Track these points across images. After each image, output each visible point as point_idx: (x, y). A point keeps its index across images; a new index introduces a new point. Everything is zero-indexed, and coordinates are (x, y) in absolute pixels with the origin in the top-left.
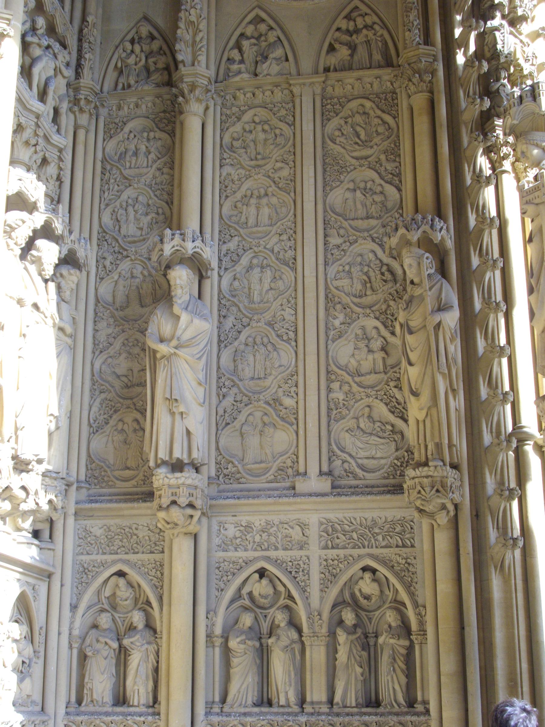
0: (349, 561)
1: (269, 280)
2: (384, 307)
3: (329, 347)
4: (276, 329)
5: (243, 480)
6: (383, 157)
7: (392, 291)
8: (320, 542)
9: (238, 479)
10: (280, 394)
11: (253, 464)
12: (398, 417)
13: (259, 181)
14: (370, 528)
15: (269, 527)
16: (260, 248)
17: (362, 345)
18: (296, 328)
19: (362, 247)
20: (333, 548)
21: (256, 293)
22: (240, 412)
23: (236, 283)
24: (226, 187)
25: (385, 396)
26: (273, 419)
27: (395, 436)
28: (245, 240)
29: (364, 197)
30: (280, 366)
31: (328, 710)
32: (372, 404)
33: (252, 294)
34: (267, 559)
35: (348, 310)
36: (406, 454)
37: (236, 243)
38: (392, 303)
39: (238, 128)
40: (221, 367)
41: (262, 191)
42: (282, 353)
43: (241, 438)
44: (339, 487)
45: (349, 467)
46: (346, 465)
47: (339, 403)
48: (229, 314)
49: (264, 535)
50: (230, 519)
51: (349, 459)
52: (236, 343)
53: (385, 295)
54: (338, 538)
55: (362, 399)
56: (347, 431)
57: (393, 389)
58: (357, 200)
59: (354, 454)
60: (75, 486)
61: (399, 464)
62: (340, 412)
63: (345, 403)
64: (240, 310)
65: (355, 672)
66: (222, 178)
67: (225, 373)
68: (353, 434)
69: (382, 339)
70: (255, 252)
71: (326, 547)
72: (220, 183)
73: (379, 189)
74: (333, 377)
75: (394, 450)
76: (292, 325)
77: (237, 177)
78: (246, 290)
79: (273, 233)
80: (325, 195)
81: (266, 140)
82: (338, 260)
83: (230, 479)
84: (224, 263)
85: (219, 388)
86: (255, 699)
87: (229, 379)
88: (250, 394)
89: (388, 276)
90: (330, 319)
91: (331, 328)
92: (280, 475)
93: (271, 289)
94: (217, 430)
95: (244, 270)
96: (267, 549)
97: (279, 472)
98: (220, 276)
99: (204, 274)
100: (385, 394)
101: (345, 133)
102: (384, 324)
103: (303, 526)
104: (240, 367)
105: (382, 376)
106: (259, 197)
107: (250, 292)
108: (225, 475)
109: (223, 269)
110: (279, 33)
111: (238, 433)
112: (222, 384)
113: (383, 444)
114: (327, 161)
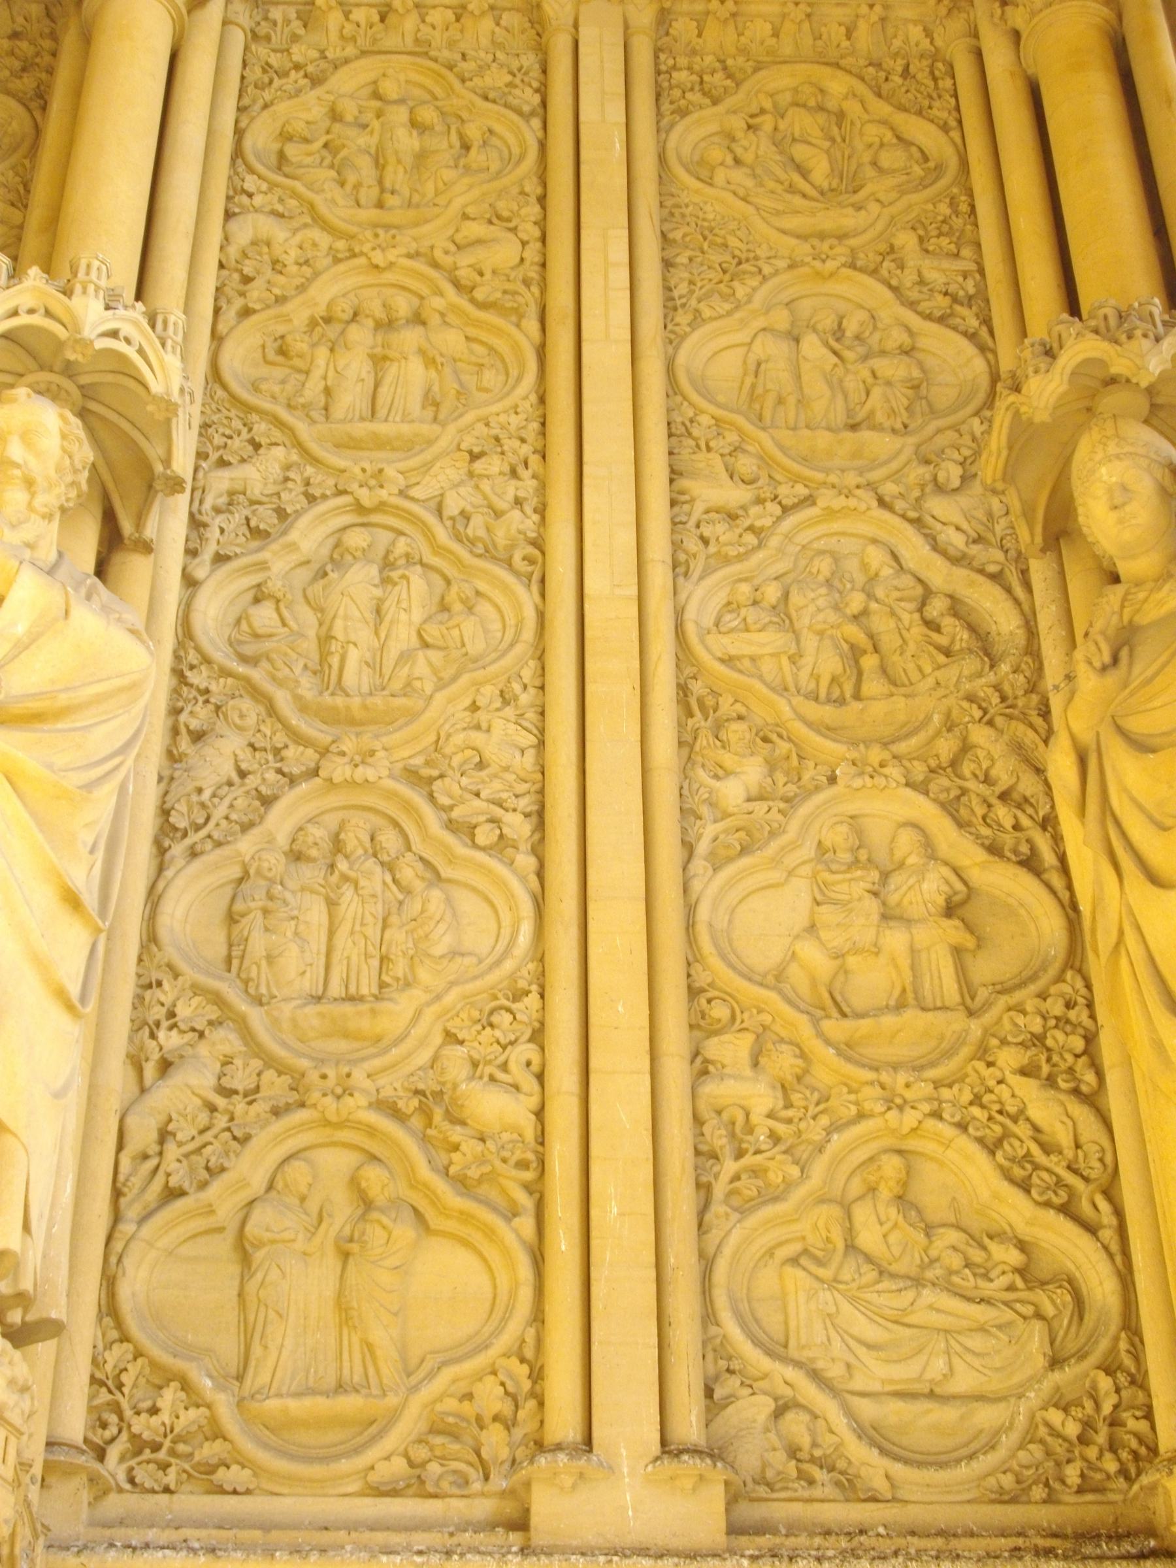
1: (417, 616)
2: (946, 747)
3: (696, 885)
4: (444, 800)
6: (907, 241)
7: (982, 687)
9: (211, 1469)
11: (298, 1395)
12: (1047, 1204)
13: (388, 277)
16: (383, 494)
17: (856, 886)
18: (542, 806)
19: (836, 526)
21: (354, 655)
22: (244, 1140)
23: (264, 616)
24: (247, 280)
25: (976, 1111)
26: (414, 1183)
27: (1041, 1297)
28: (315, 461)
29: (835, 359)
30: (455, 953)
32: (912, 1144)
33: (335, 661)
35: (783, 747)
36: (1105, 1383)
37: (276, 471)
38: (980, 735)
40: (163, 934)
42: (468, 904)
43: (235, 1269)
44: (760, 1529)
45: (812, 1432)
46: (795, 1425)
47: (750, 1129)
48: (221, 726)
51: (809, 1392)
52: (246, 845)
53: (951, 701)
55: (861, 1116)
56: (794, 1261)
57: (1015, 1080)
58: (805, 367)
59: (835, 1372)
61: (1072, 1429)
62: (756, 1172)
63: (781, 1129)
64: (272, 711)
66: (233, 251)
67: (182, 966)
68: (821, 1272)
69: (946, 872)
70: (359, 508)
72: (221, 266)
73: (898, 337)
74: (720, 1012)
75: (1041, 1362)
76: (524, 787)
77: (294, 253)
78: (310, 646)
79: (443, 443)
80: (673, 340)
81: (421, 157)
82: (727, 561)
83: (164, 1467)
84: (213, 534)
85: (144, 1027)
87: (197, 989)
88: (304, 1063)
89: (955, 632)
90: (702, 775)
91: (704, 810)
92: (443, 1459)
93: (426, 645)
94: (117, 1217)
95: (304, 574)
97: (438, 1440)
98: (190, 582)
99: (127, 526)
100: (977, 1100)
101: (748, 158)
102: (951, 808)
104: (258, 944)
105: (957, 1022)
106: (386, 325)
107: (324, 656)
108: (139, 1445)
109: (207, 555)
111: (223, 1245)
112: (158, 1013)
113: (982, 1329)
114: (677, 235)
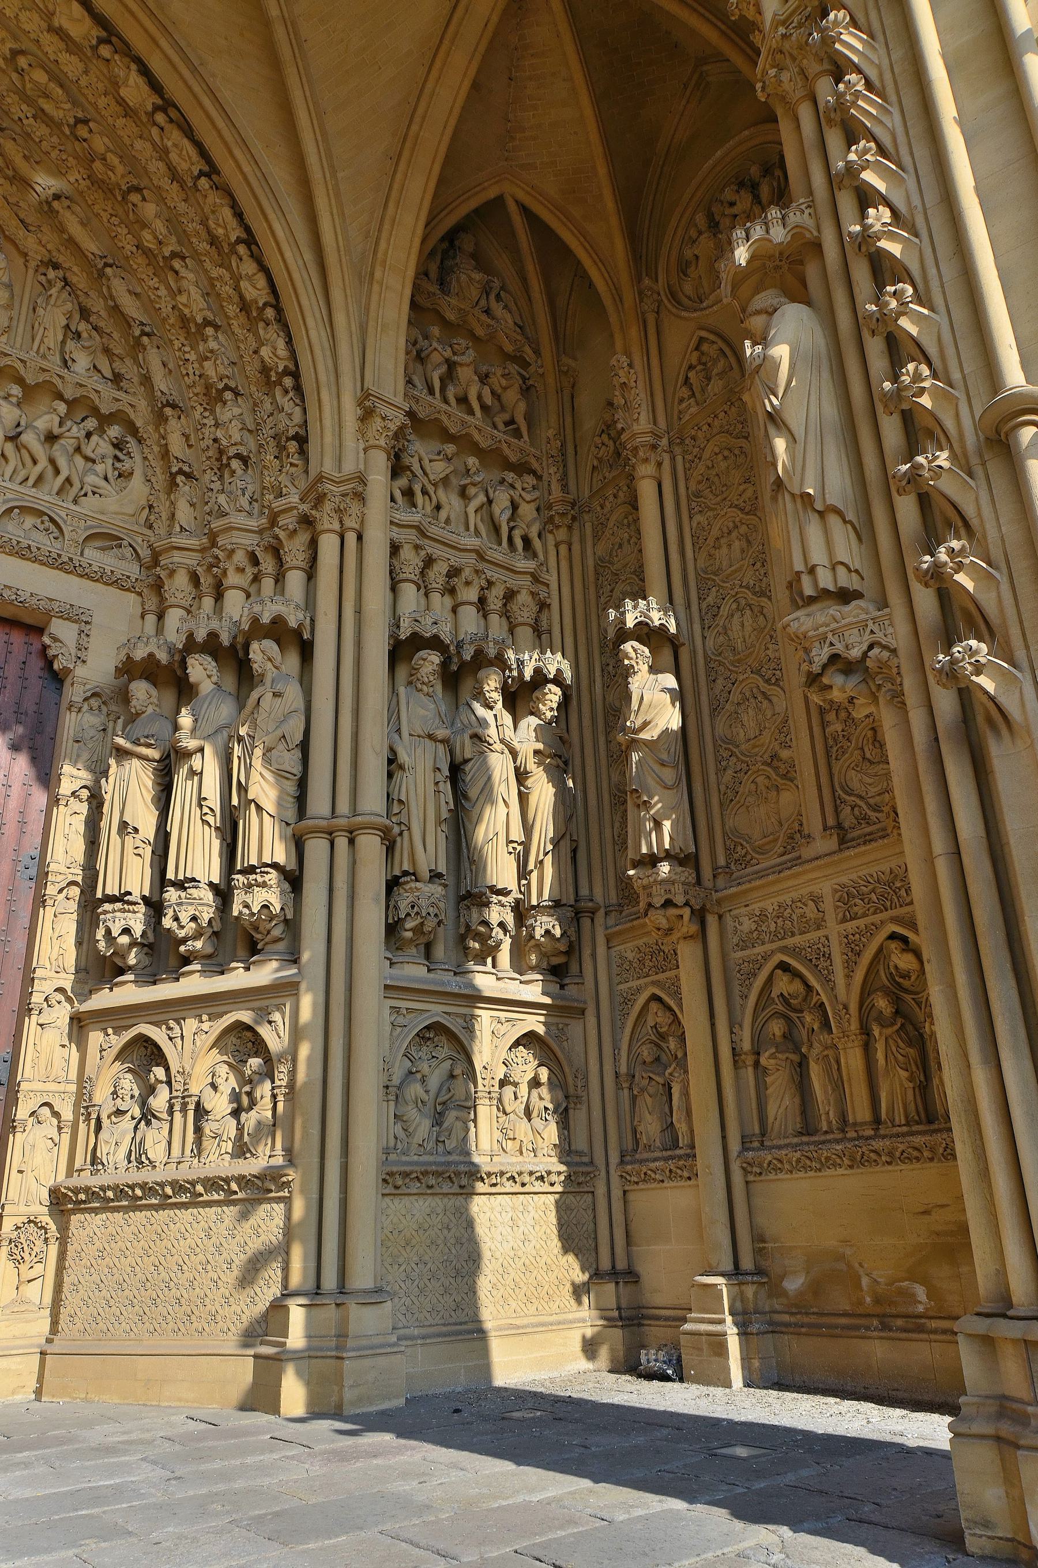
0: (871, 931)
5: (754, 861)
8: (837, 915)
10: (777, 747)
14: (890, 884)
15: (782, 910)
20: (852, 919)
31: (872, 1133)
34: (784, 950)
39: (701, 468)
41: (731, 525)
49: (780, 921)
50: (743, 910)
54: (856, 905)
60: (602, 911)
62: (842, 747)
65: (900, 1078)
71: (844, 920)
86: (798, 1126)
96: (783, 938)
103: (816, 900)
110: (721, 344)
